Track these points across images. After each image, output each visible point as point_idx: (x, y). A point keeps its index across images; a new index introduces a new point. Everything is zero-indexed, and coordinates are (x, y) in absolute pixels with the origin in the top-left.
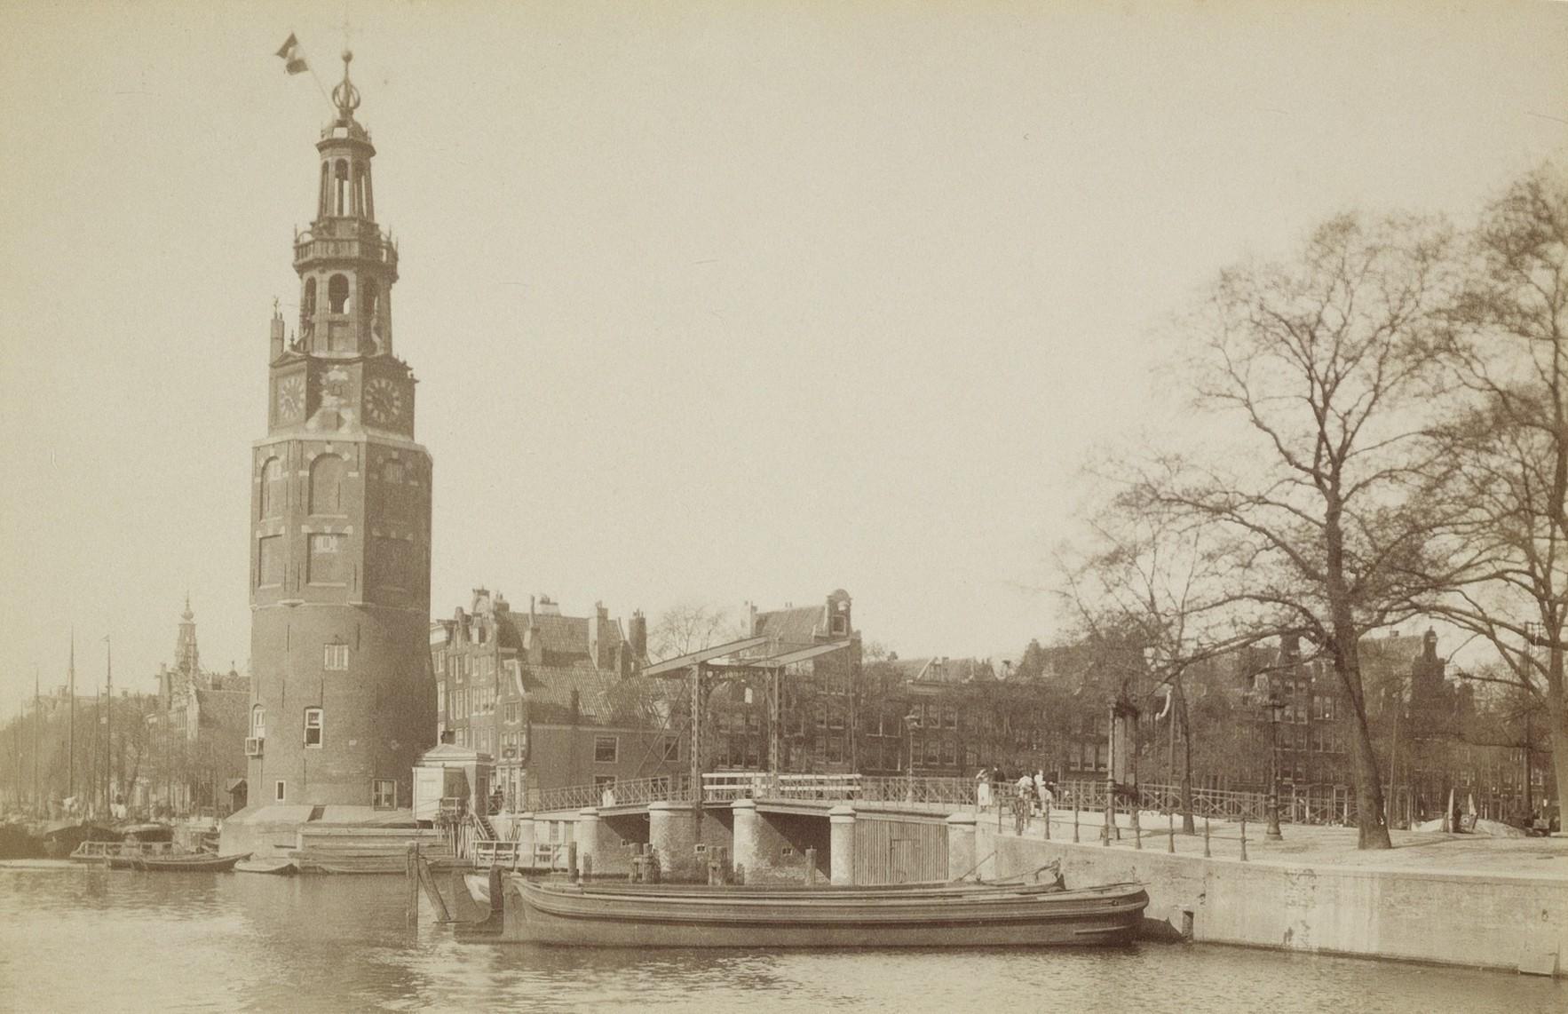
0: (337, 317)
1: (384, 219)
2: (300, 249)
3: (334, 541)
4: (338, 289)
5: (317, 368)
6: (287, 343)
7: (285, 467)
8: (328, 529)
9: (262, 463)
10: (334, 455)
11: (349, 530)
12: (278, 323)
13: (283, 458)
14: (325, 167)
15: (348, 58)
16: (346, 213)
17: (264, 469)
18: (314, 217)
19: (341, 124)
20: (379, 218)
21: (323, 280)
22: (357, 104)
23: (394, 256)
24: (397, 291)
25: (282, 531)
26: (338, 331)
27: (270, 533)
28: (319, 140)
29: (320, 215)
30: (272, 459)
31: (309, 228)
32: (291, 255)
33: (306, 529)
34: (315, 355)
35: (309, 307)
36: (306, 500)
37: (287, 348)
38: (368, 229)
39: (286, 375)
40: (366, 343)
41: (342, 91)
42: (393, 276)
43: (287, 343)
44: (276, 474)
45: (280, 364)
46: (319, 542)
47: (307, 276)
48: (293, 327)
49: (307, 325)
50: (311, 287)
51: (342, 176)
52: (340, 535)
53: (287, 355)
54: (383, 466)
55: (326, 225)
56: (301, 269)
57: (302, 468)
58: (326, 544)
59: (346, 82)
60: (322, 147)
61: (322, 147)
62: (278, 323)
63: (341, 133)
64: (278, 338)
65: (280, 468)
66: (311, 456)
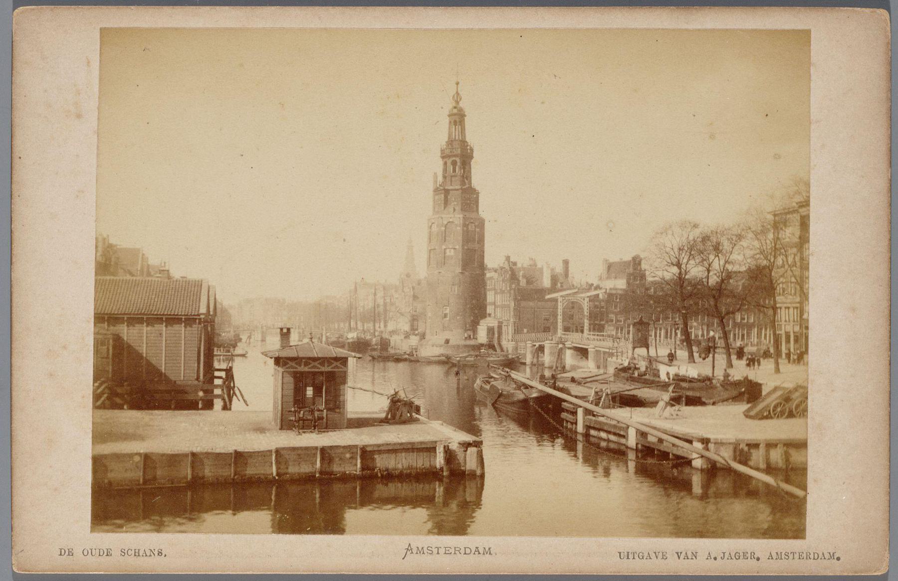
0: (453, 174)
1: (468, 139)
2: (442, 151)
3: (452, 250)
4: (454, 163)
5: (447, 192)
6: (438, 184)
7: (437, 226)
8: (451, 247)
9: (430, 224)
10: (452, 222)
11: (457, 247)
12: (435, 174)
13: (436, 223)
14: (450, 122)
15: (457, 84)
16: (457, 138)
17: (431, 226)
18: (446, 139)
19: (455, 108)
20: (467, 140)
21: (449, 162)
22: (461, 99)
23: (472, 150)
24: (473, 162)
25: (437, 248)
26: (453, 179)
27: (433, 248)
28: (448, 113)
29: (449, 139)
30: (433, 223)
31: (445, 143)
32: (439, 154)
33: (444, 247)
34: (446, 188)
35: (445, 170)
36: (444, 237)
37: (438, 186)
38: (463, 143)
39: (436, 195)
40: (463, 183)
41: (456, 96)
42: (472, 157)
43: (438, 184)
44: (435, 228)
45: (436, 190)
46: (448, 251)
47: (445, 160)
48: (440, 179)
49: (445, 177)
50: (445, 164)
51: (455, 125)
52: (455, 249)
53: (438, 188)
54: (468, 224)
55: (450, 142)
56: (443, 158)
57: (442, 226)
58: (450, 252)
59: (457, 93)
60: (449, 116)
61: (449, 116)
62: (435, 174)
63: (455, 111)
64: (436, 182)
65: (435, 227)
66: (445, 223)
